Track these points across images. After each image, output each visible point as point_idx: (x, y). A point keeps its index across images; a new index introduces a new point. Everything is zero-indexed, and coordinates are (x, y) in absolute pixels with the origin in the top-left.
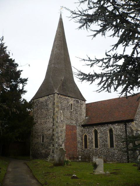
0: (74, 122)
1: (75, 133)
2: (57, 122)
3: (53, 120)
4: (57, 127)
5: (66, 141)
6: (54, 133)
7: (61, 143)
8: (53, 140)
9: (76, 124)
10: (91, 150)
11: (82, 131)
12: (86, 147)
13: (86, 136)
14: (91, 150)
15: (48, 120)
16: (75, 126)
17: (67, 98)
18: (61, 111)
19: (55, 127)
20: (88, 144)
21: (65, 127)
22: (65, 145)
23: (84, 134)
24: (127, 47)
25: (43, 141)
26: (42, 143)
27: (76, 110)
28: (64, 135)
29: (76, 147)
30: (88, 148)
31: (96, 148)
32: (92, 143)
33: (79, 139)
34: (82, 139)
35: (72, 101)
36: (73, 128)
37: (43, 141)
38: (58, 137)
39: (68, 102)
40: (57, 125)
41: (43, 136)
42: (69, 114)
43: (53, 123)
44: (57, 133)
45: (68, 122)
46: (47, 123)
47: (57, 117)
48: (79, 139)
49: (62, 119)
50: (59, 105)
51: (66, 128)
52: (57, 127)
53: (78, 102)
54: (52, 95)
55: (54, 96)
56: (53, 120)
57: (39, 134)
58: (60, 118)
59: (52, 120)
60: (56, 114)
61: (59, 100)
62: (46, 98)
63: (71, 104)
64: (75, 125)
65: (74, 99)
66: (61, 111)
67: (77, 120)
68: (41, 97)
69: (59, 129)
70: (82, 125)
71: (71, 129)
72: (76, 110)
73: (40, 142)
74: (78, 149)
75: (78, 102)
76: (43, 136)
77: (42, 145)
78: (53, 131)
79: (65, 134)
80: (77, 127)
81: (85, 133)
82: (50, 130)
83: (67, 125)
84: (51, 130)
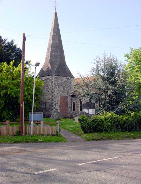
0: (66, 94)
1: (67, 101)
2: (55, 95)
3: (52, 93)
4: (55, 98)
5: (61, 107)
6: (53, 102)
7: (57, 108)
8: (52, 106)
9: (67, 95)
10: (77, 112)
11: (71, 100)
12: (74, 110)
13: (74, 103)
14: (77, 112)
15: (48, 93)
16: (66, 96)
17: (61, 77)
18: (57, 87)
19: (53, 98)
20: (75, 108)
21: (60, 98)
22: (60, 109)
23: (73, 102)
24: (37, 67)
25: (45, 107)
26: (44, 108)
27: (67, 85)
28: (59, 102)
29: (67, 111)
30: (75, 111)
31: (81, 111)
32: (78, 107)
33: (69, 105)
34: (71, 105)
35: (64, 79)
36: (66, 97)
37: (45, 107)
38: (55, 105)
39: (62, 80)
40: (55, 96)
41: (45, 104)
42: (63, 88)
43: (52, 95)
44: (55, 101)
45: (62, 95)
46: (48, 95)
47: (55, 91)
48: (69, 105)
49: (58, 92)
50: (56, 83)
51: (61, 98)
52: (55, 98)
53: (68, 79)
54: (51, 76)
55: (52, 77)
56: (52, 93)
57: (42, 102)
58: (57, 92)
59: (51, 93)
60: (54, 89)
61: (56, 79)
62: (47, 77)
63: (64, 82)
64: (67, 95)
65: (66, 78)
66: (57, 87)
67: (68, 92)
68: (43, 77)
69: (56, 99)
70: (71, 96)
71: (64, 98)
72: (67, 85)
73: (43, 107)
74: (69, 112)
75: (68, 79)
76: (45, 104)
77: (45, 109)
78: (52, 100)
79: (60, 102)
80: (68, 97)
81: (73, 101)
82: (50, 99)
83: (61, 96)
84: (51, 100)
